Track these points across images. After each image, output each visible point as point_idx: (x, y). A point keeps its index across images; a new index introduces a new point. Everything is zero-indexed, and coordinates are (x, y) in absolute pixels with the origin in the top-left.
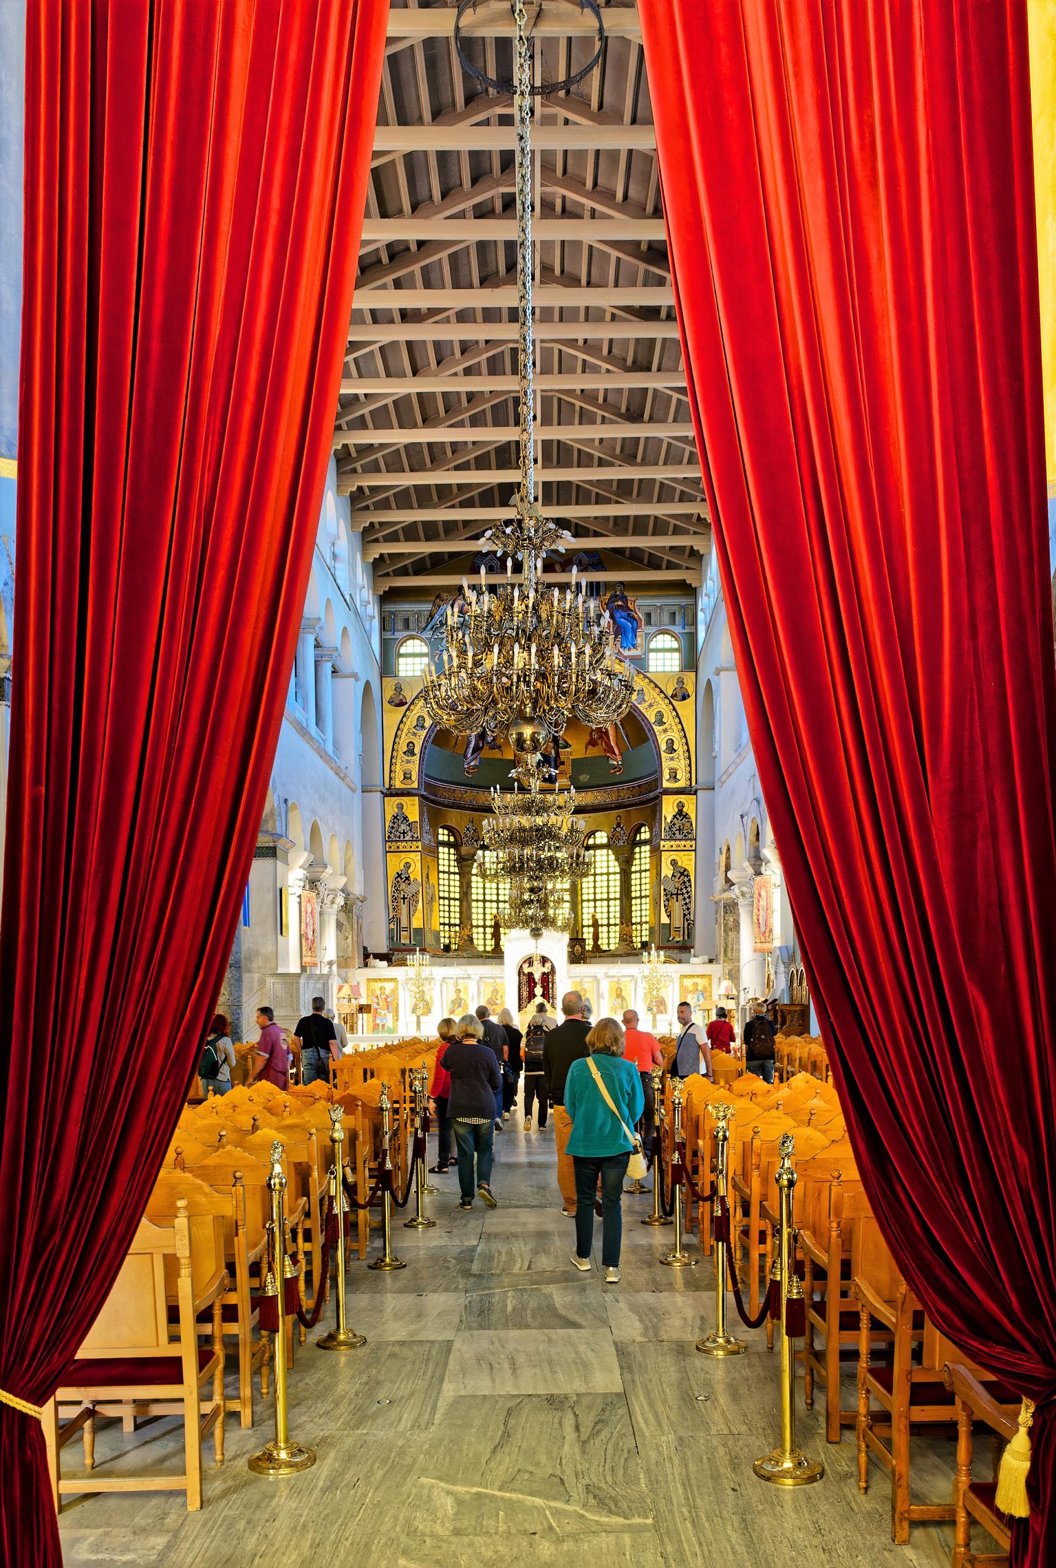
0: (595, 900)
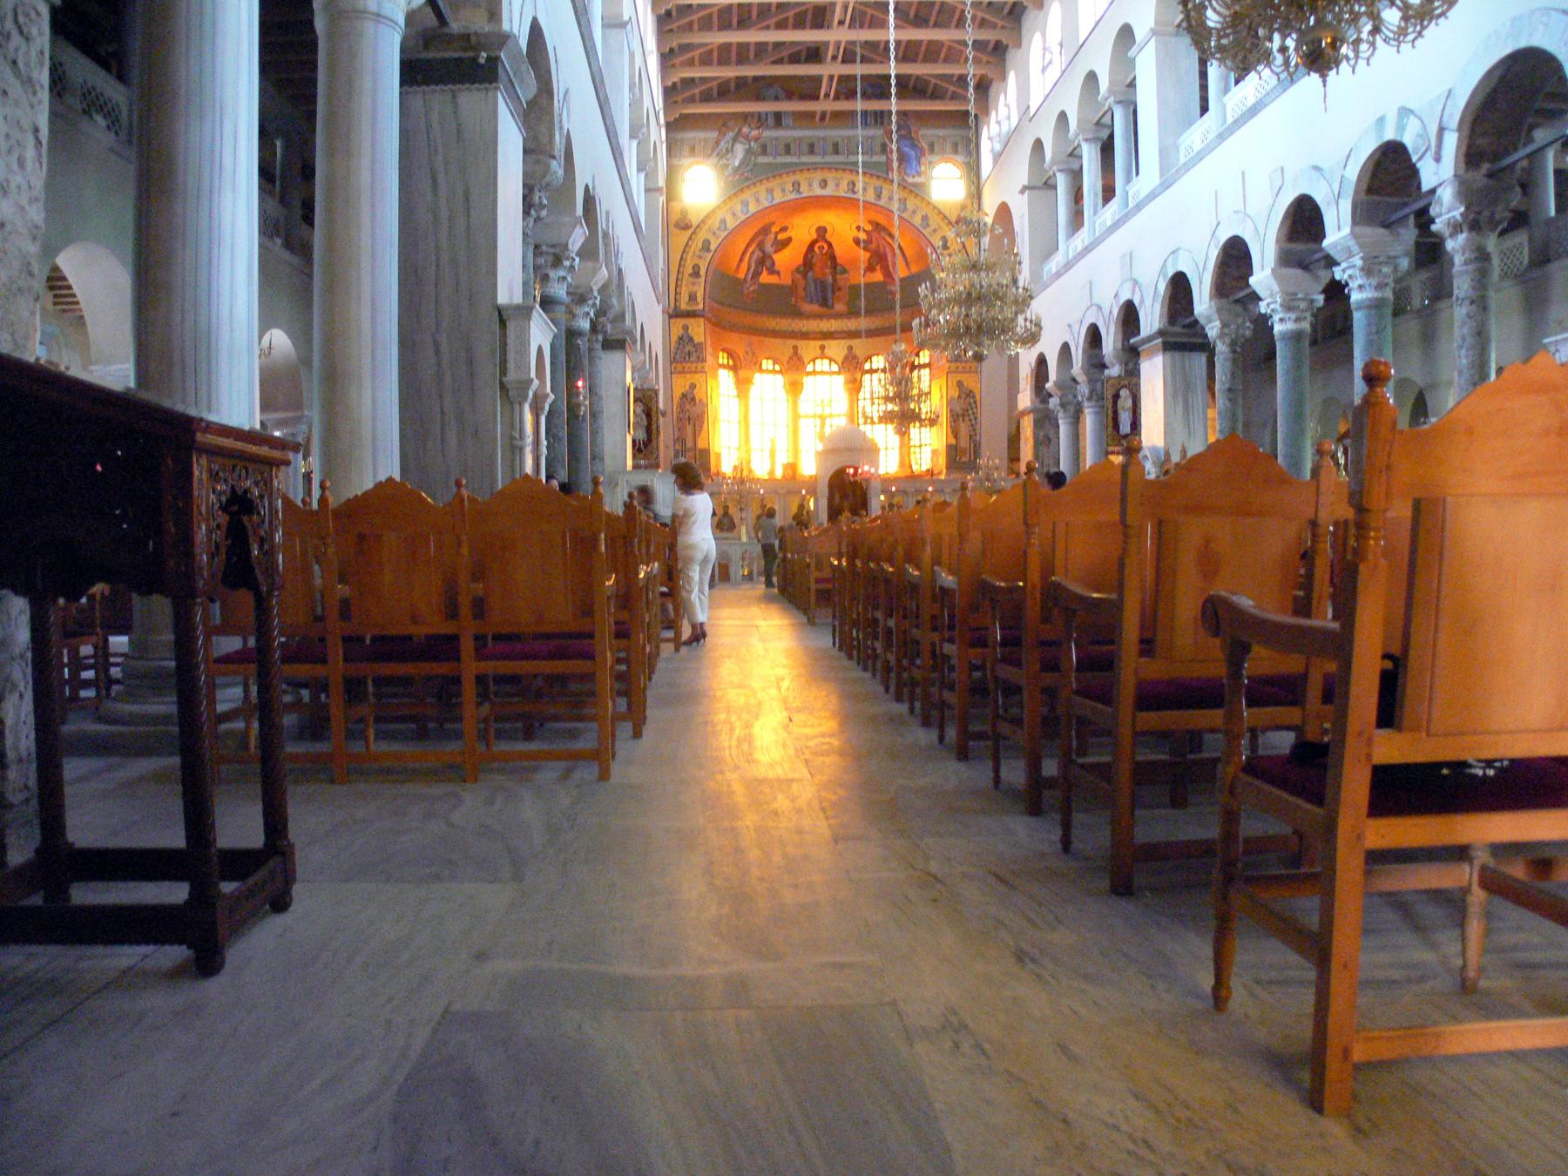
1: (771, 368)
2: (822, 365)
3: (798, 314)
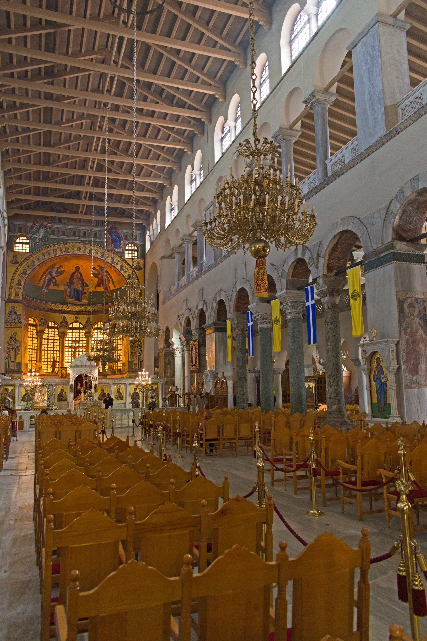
0: (48, 350)
1: (53, 325)
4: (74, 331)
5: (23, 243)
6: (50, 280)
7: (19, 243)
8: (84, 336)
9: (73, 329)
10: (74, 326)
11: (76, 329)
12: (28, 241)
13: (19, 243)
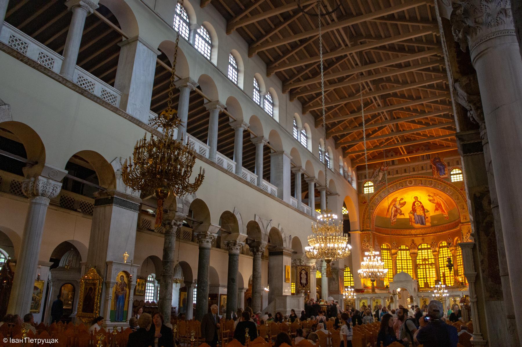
1: (404, 248)
2: (424, 246)
3: (414, 228)
4: (423, 251)
5: (457, 174)
6: (396, 211)
7: (454, 174)
8: (432, 255)
9: (422, 249)
10: (423, 247)
11: (424, 249)
12: (460, 172)
13: (454, 174)
